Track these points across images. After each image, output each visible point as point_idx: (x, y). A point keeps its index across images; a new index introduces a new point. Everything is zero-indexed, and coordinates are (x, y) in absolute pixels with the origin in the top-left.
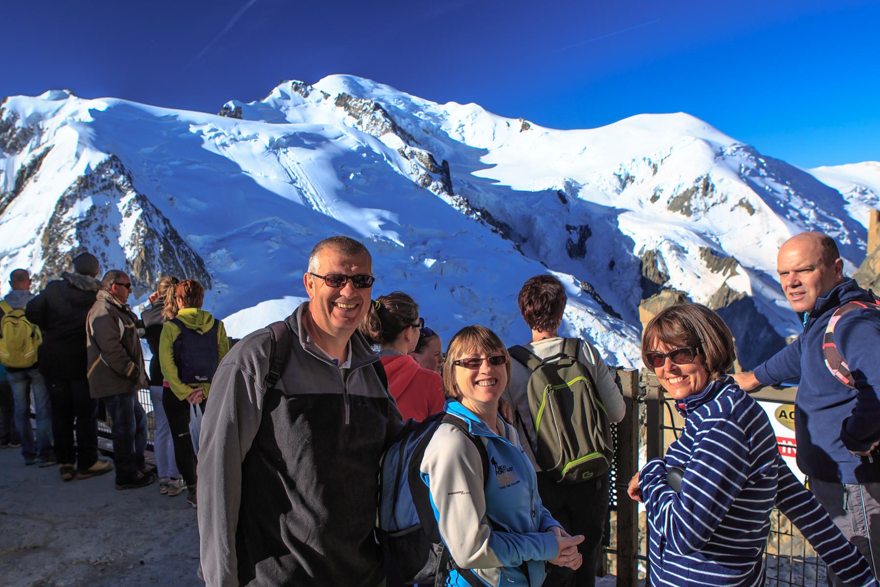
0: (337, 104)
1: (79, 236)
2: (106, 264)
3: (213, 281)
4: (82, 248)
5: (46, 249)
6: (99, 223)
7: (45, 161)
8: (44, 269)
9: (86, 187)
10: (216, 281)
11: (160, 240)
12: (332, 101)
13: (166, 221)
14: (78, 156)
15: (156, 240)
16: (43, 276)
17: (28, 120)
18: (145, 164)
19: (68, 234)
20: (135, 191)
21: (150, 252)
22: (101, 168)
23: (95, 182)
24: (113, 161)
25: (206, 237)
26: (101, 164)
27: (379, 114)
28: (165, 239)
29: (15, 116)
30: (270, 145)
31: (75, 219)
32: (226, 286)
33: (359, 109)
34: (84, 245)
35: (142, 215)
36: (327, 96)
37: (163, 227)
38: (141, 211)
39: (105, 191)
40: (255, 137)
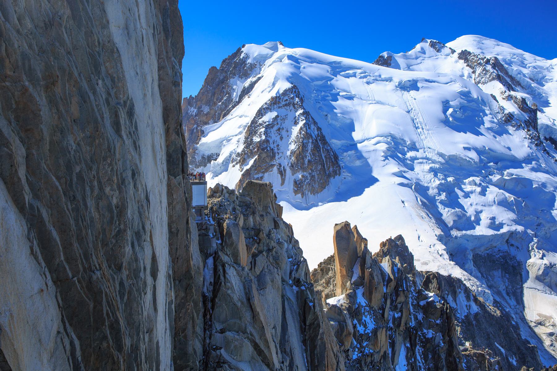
0: (460, 58)
1: (266, 133)
2: (279, 151)
3: (342, 170)
4: (266, 141)
5: (246, 138)
6: (279, 126)
7: (256, 85)
8: (243, 151)
9: (275, 103)
11: (313, 140)
12: (456, 55)
14: (274, 84)
16: (242, 154)
17: (254, 59)
18: (315, 92)
19: (260, 131)
20: (304, 109)
21: (306, 147)
22: (286, 92)
23: (281, 101)
24: (294, 90)
25: (343, 142)
26: (286, 91)
27: (489, 67)
29: (247, 57)
30: (398, 85)
31: (265, 123)
32: (349, 175)
33: (475, 62)
34: (268, 138)
35: (304, 124)
36: (453, 51)
37: (316, 133)
38: (304, 121)
39: (285, 107)
40: (390, 80)
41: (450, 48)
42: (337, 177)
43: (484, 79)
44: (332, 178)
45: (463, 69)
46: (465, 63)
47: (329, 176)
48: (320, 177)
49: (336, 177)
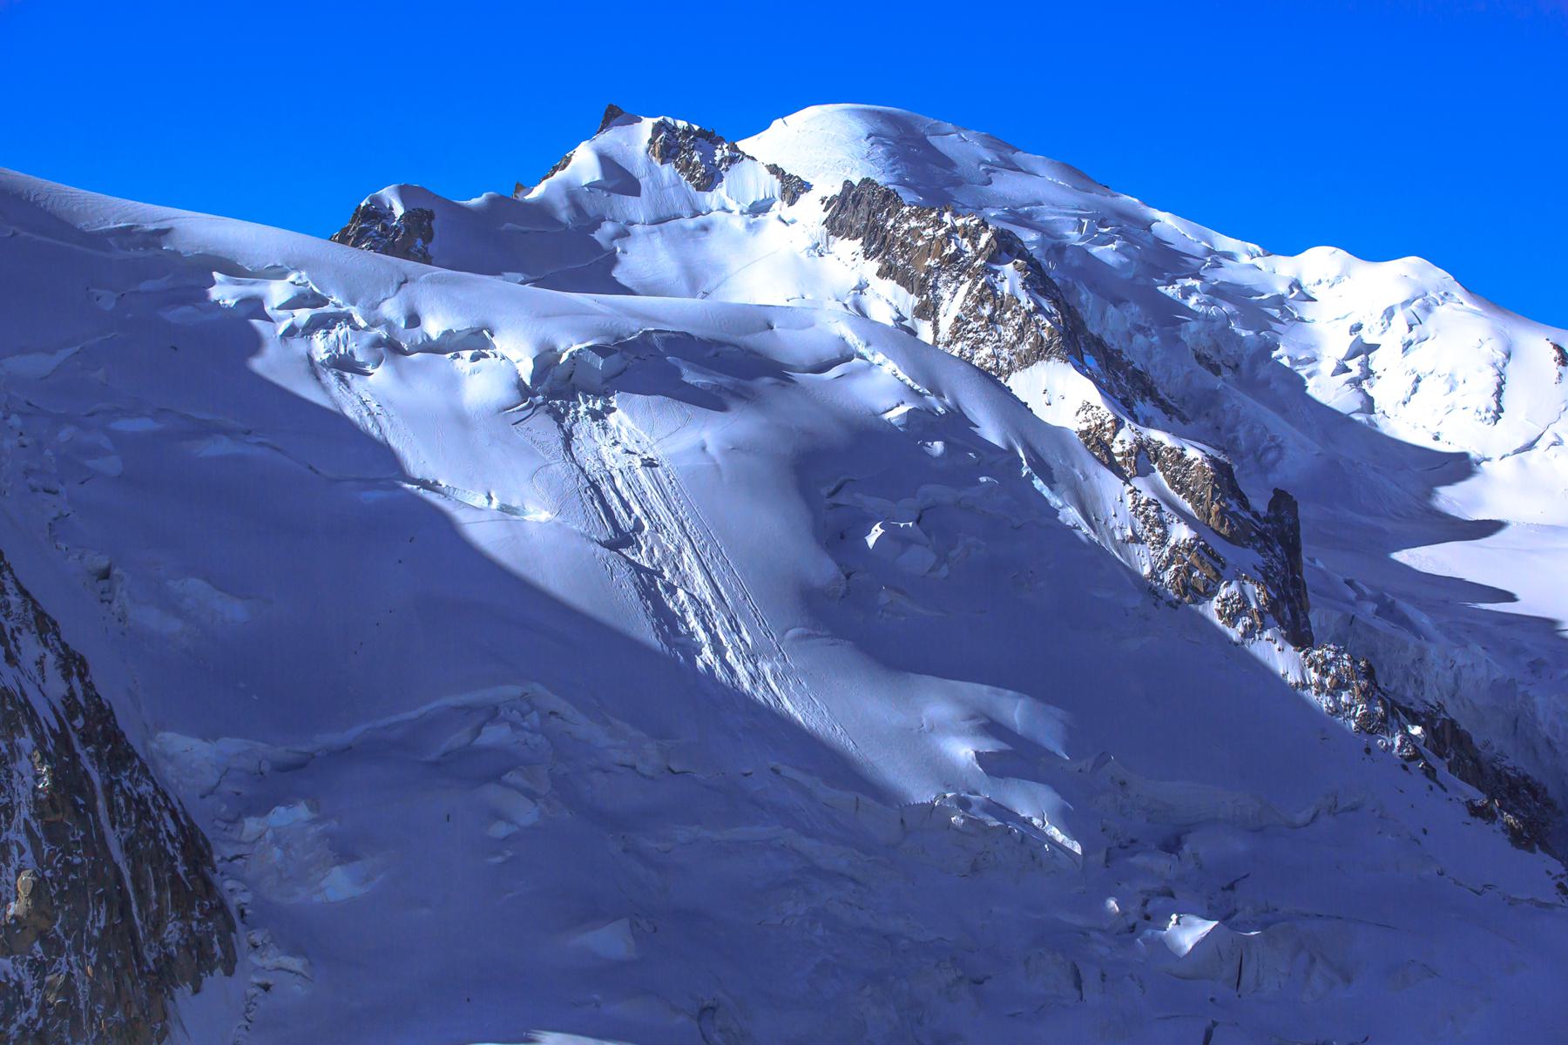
0: (836, 226)
10: (257, 937)
11: (40, 740)
12: (811, 211)
13: (73, 664)
15: (26, 741)
18: (15, 420)
25: (231, 745)
27: (1010, 278)
28: (63, 739)
30: (536, 377)
32: (296, 963)
33: (927, 251)
36: (794, 188)
37: (57, 687)
40: (477, 341)
41: (774, 170)
42: (214, 981)
43: (986, 351)
44: (183, 992)
45: (861, 288)
46: (868, 255)
47: (163, 977)
48: (108, 985)
49: (208, 981)
